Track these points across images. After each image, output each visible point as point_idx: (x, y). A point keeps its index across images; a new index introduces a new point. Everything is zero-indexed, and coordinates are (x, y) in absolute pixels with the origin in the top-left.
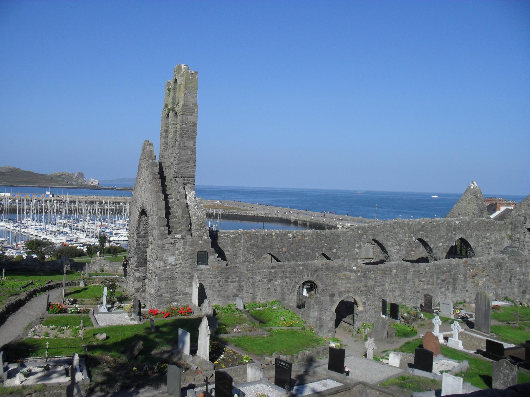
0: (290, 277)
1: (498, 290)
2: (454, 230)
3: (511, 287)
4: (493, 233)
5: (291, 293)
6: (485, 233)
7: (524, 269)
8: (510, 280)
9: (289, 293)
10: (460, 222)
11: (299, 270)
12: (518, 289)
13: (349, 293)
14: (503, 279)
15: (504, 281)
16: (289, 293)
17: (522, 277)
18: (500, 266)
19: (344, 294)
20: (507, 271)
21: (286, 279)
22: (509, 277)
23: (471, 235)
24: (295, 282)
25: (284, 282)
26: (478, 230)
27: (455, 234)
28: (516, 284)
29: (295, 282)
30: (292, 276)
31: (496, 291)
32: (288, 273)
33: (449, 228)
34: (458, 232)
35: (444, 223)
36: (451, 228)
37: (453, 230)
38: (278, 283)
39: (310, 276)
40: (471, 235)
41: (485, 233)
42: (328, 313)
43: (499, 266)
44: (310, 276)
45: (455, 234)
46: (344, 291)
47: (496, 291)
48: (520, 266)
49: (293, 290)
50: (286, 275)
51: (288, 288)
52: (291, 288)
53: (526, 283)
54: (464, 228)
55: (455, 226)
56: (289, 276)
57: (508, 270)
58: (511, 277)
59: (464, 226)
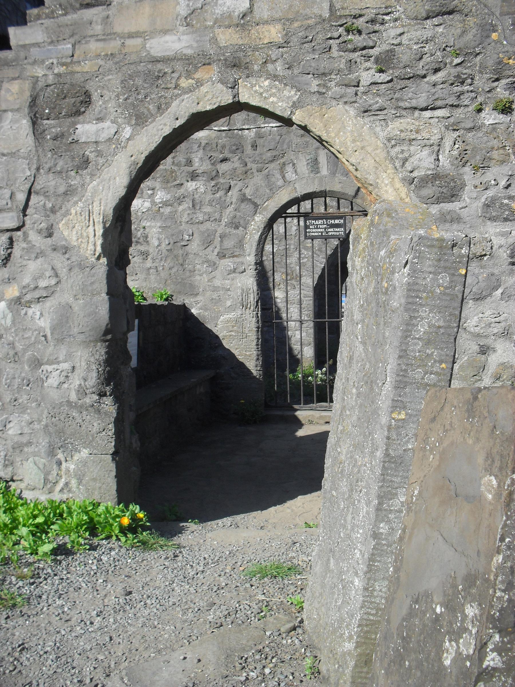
0: (214, 176)
5: (222, 255)
9: (213, 257)
11: (259, 136)
13: (235, 74)
16: (213, 257)
19: (184, 83)
21: (191, 186)
24: (243, 199)
25: (180, 200)
29: (243, 199)
30: (224, 167)
32: (200, 154)
38: (147, 204)
39: (324, 171)
42: (33, 266)
44: (324, 171)
46: (187, 60)
49: (229, 243)
50: (189, 162)
51: (203, 228)
52: (220, 231)
56: (206, 166)
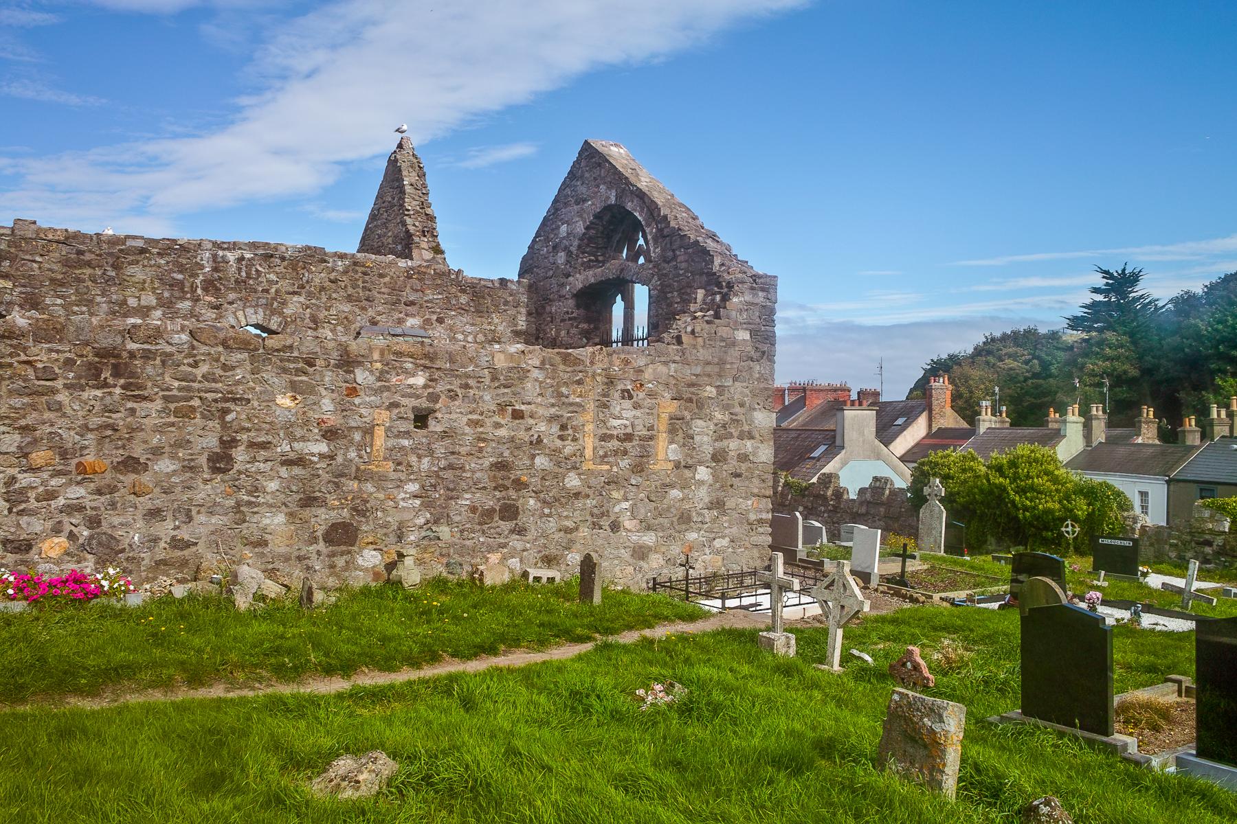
1: (112, 520)
2: (209, 285)
3: (232, 503)
4: (440, 321)
6: (397, 315)
7: (327, 404)
8: (220, 462)
10: (248, 256)
12: (291, 515)
14: (157, 452)
15: (165, 465)
17: (323, 447)
18: (117, 374)
20: (193, 409)
22: (211, 442)
23: (314, 319)
26: (349, 298)
27: (217, 307)
28: (273, 486)
31: (94, 522)
33: (180, 277)
34: (232, 296)
35: (142, 251)
36: (195, 276)
37: (205, 289)
40: (314, 319)
41: (397, 315)
43: (106, 374)
45: (217, 307)
47: (94, 522)
48: (294, 387)
53: (355, 485)
54: (270, 282)
55: (215, 269)
57: (196, 403)
58: (229, 444)
59: (273, 277)
